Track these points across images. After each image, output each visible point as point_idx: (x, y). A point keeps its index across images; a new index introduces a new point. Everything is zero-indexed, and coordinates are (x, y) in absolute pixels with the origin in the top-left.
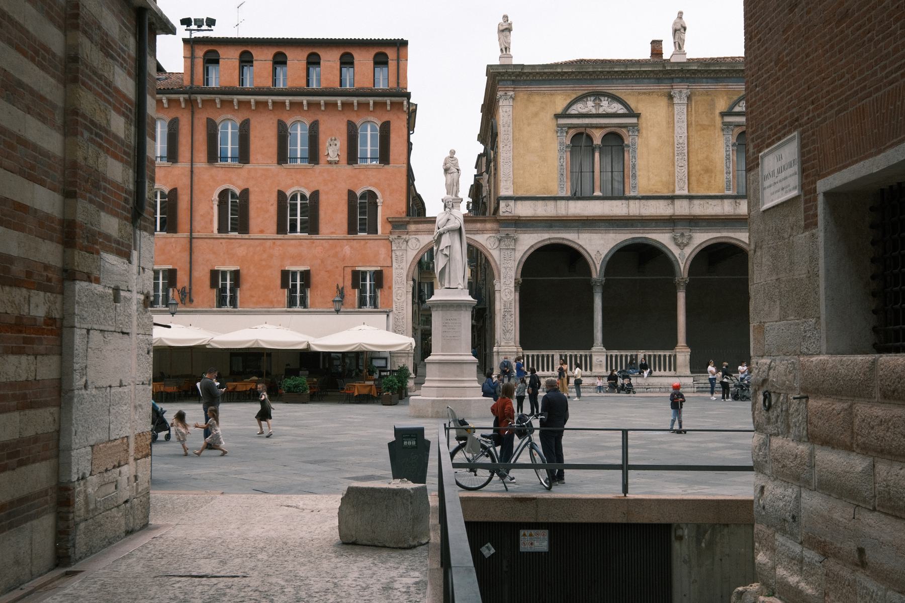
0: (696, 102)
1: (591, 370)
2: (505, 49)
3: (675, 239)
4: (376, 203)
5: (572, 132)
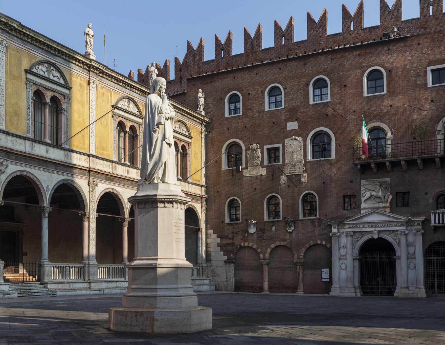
0: (10, 54)
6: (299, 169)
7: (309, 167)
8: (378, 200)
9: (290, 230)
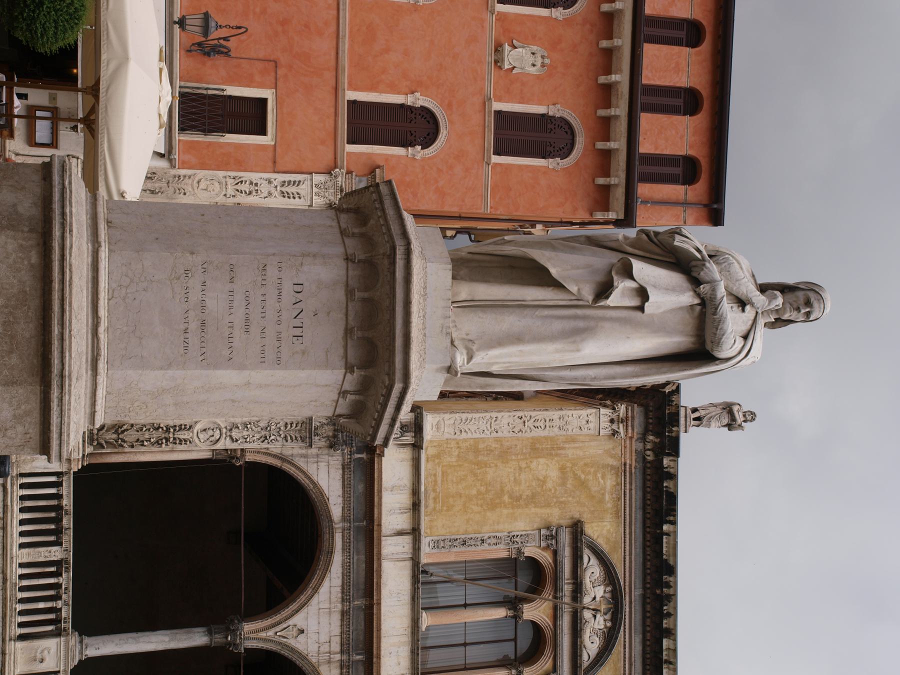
1: (22, 637)
4: (412, 145)
5: (545, 558)
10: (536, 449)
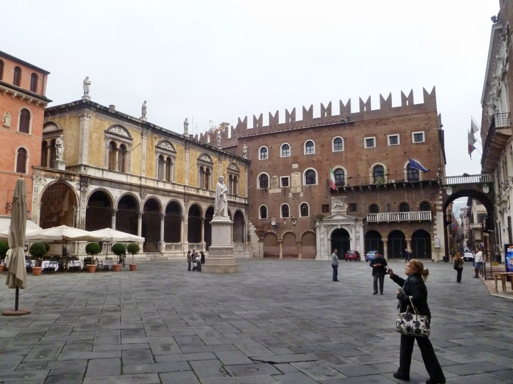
2: (86, 92)
3: (141, 195)
5: (110, 140)
6: (299, 190)
7: (304, 189)
8: (340, 208)
9: (294, 224)
10: (90, 138)
